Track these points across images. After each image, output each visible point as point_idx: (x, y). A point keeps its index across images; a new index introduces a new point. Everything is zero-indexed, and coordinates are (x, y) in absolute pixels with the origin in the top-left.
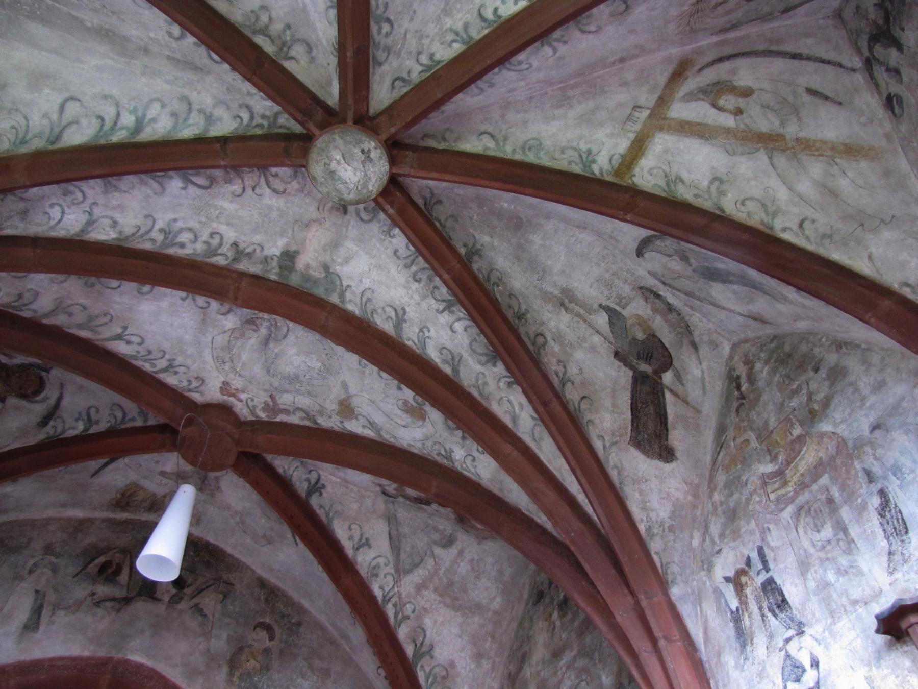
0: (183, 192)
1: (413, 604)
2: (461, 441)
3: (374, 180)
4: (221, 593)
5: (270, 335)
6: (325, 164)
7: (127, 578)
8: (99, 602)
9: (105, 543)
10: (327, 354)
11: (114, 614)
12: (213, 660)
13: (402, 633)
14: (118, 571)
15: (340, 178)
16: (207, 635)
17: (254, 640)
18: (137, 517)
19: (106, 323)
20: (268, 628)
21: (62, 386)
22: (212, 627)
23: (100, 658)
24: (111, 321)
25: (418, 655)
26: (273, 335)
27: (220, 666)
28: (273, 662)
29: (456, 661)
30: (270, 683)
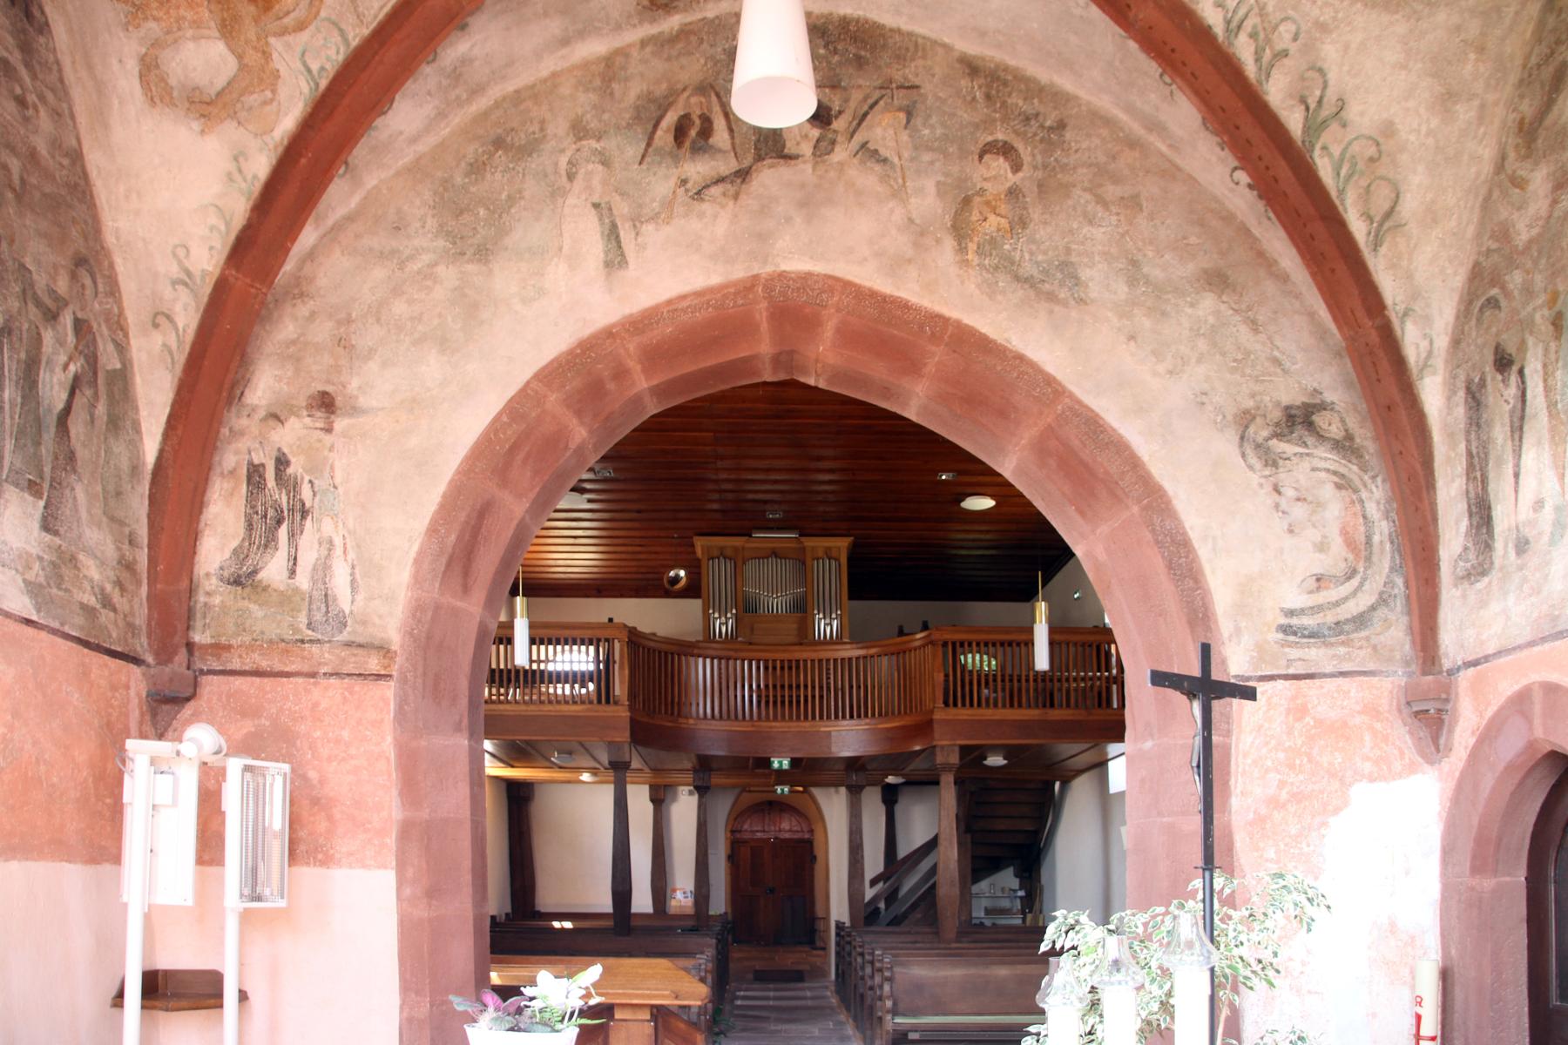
1: (1294, 22)
4: (900, 109)
7: (726, 135)
8: (699, 193)
9: (664, 86)
11: (731, 203)
12: (922, 234)
13: (1276, 93)
14: (706, 131)
16: (899, 194)
17: (985, 179)
18: (699, 16)
20: (1006, 150)
22: (903, 179)
23: (734, 284)
25: (1314, 127)
27: (938, 241)
28: (1030, 211)
29: (1397, 121)
30: (1034, 247)
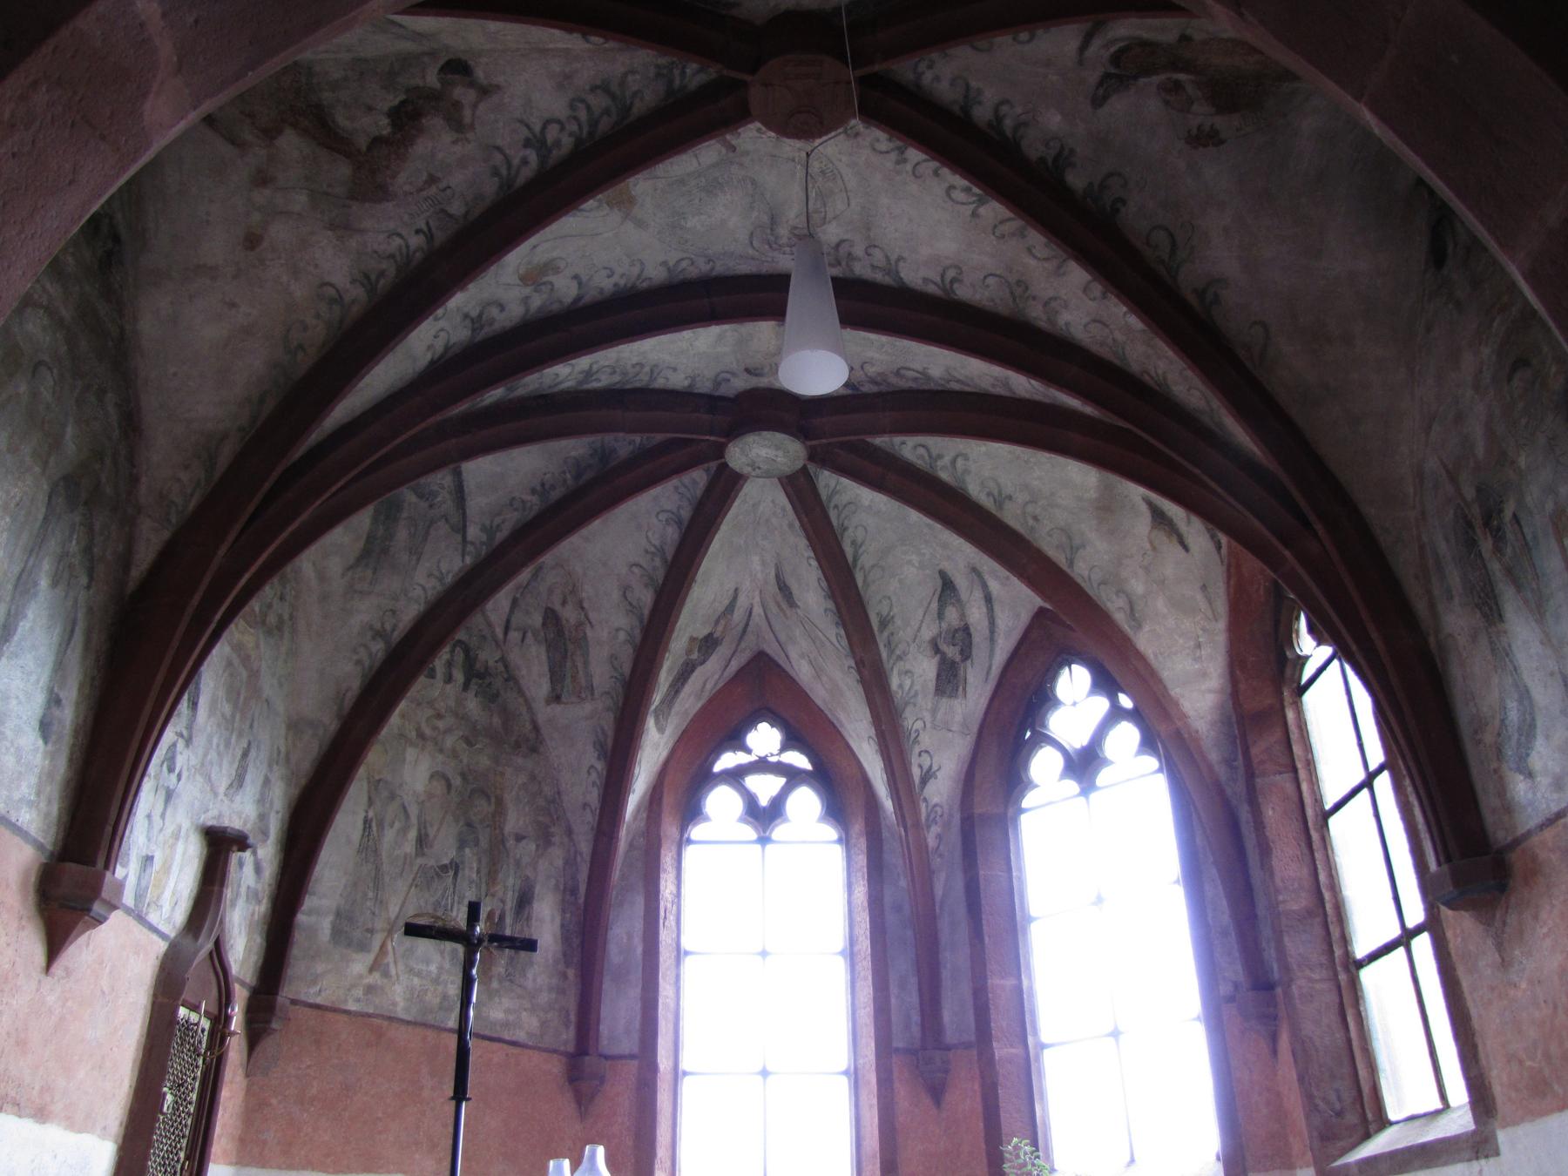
0: (925, 366)
2: (466, 310)
3: (737, 455)
5: (772, 230)
6: (788, 452)
10: (686, 241)
15: (770, 447)
19: (1001, 222)
21: (1081, 62)
24: (995, 227)
26: (769, 231)
